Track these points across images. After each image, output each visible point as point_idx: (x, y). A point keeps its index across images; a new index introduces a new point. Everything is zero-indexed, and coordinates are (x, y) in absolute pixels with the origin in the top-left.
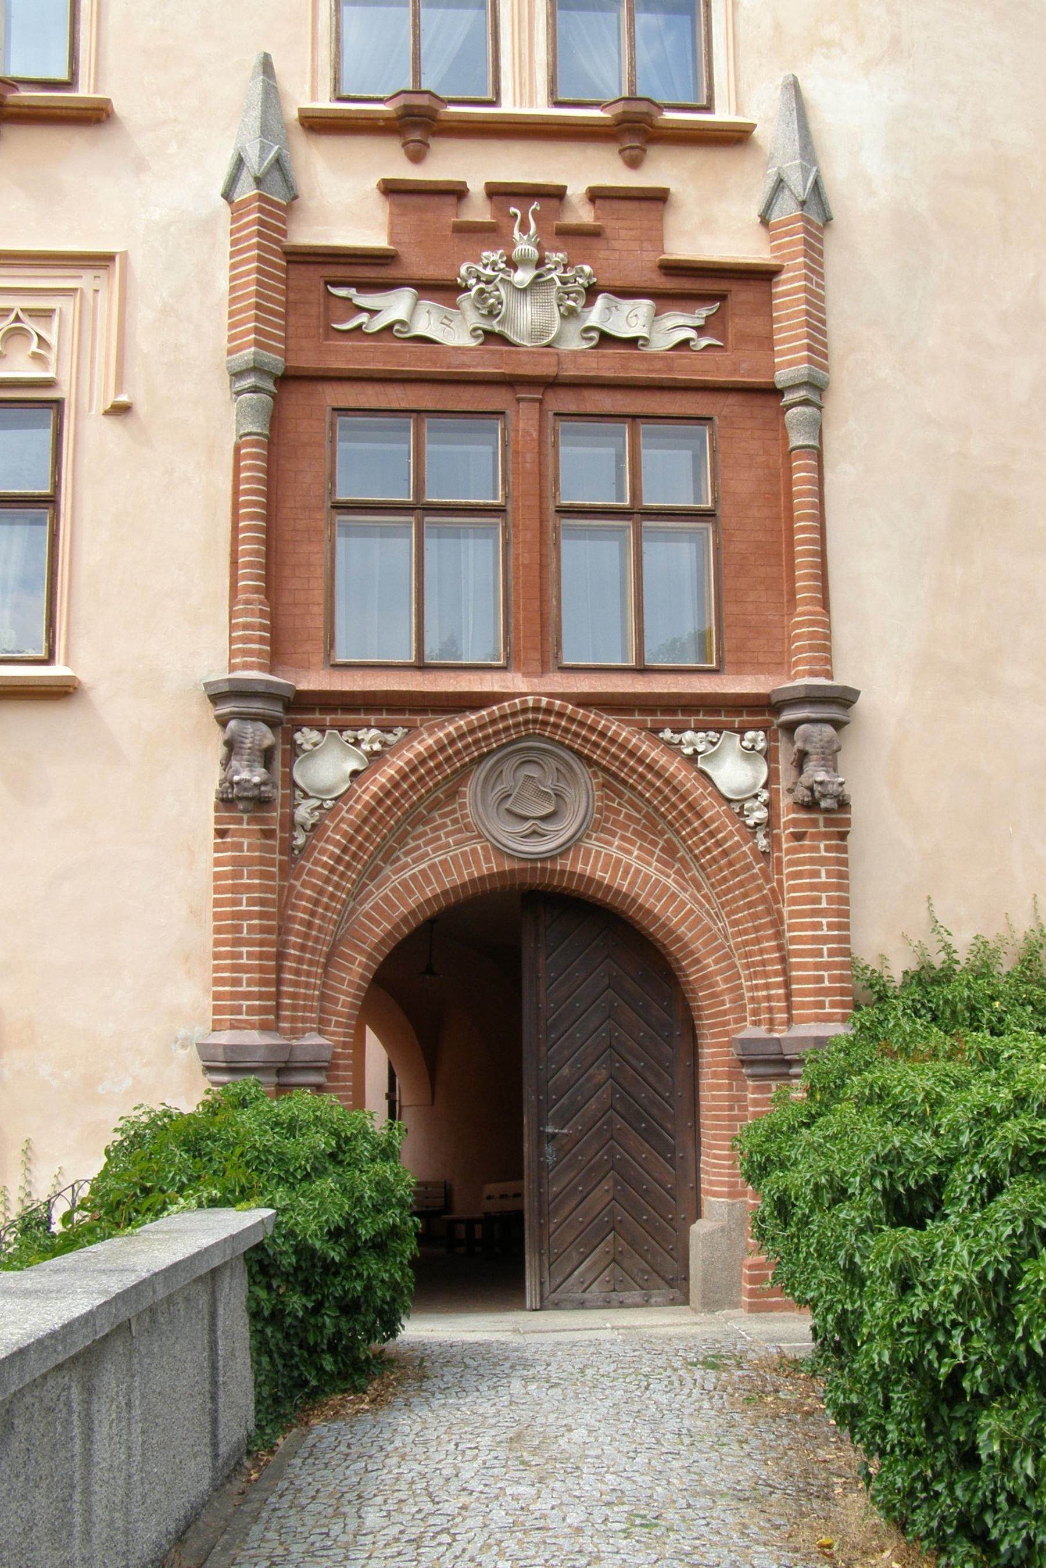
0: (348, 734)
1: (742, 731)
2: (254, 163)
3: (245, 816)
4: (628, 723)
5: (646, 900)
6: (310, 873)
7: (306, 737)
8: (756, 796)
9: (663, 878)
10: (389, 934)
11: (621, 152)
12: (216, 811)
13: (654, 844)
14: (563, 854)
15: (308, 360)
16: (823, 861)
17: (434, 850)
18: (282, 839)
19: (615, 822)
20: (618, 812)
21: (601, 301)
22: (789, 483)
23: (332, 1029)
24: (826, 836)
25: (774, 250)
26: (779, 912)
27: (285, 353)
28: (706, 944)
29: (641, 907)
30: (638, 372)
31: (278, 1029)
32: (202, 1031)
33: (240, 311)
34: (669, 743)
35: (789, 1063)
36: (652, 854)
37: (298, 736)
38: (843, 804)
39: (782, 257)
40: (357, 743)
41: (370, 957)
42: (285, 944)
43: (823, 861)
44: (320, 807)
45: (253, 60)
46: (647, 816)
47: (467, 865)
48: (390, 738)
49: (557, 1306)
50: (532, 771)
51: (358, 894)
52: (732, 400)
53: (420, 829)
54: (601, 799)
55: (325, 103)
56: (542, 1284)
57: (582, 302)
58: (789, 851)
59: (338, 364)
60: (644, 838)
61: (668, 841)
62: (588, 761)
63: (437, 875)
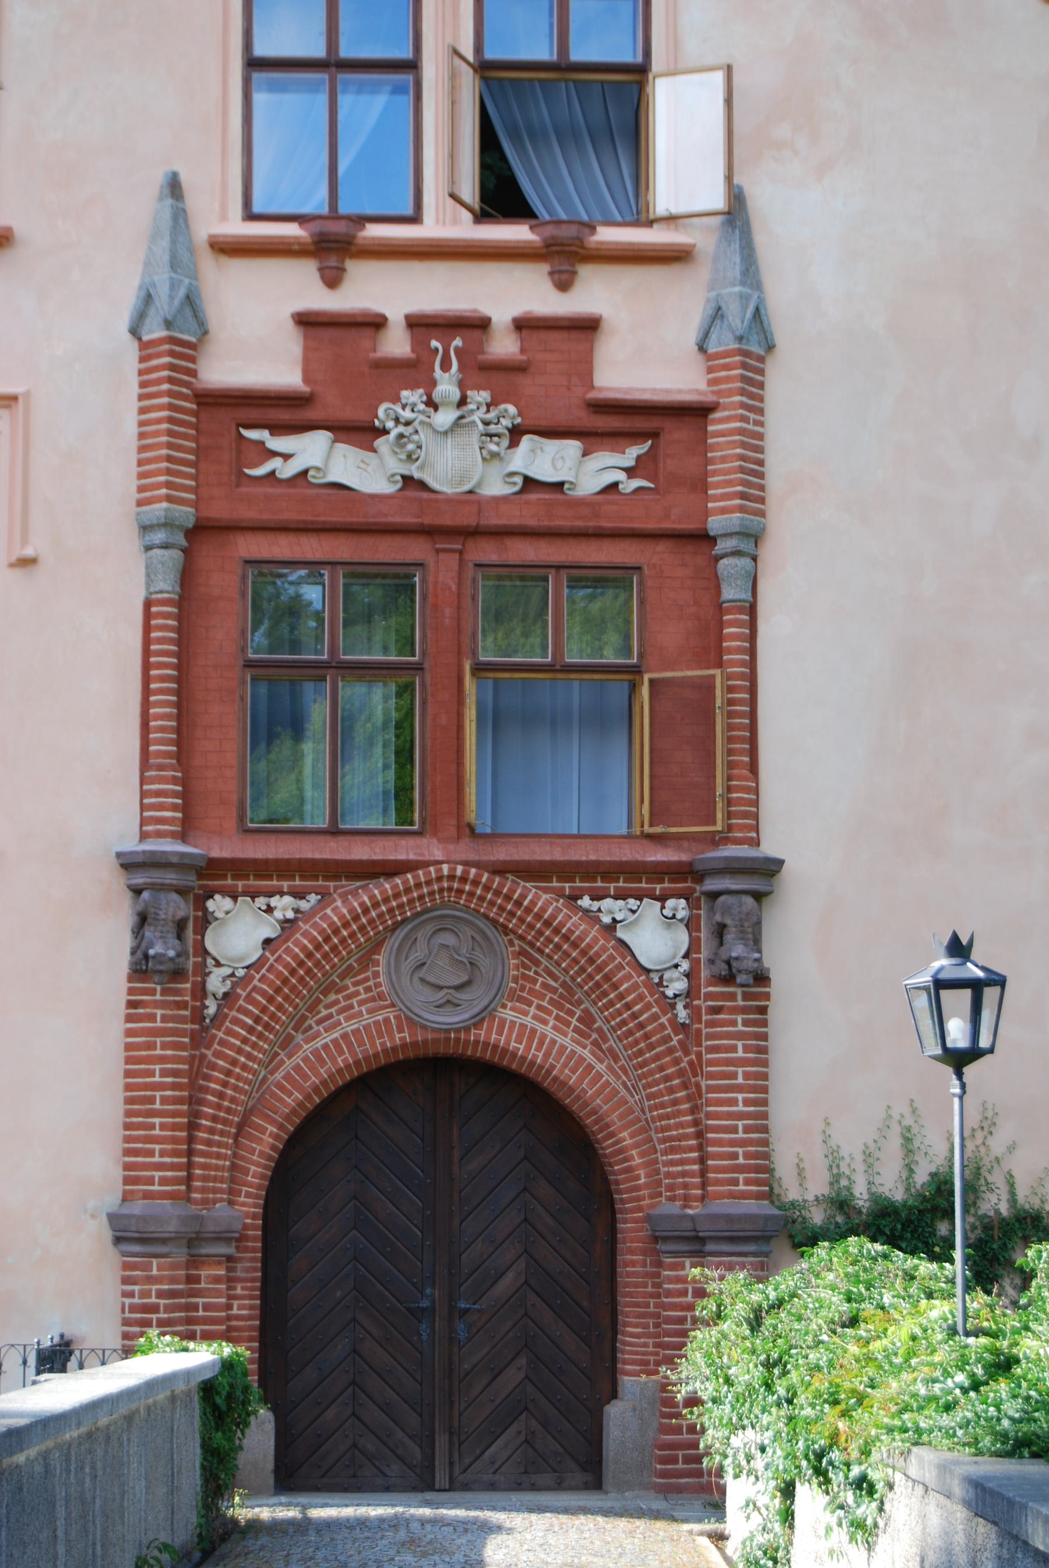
0: (261, 901)
1: (662, 899)
2: (164, 305)
3: (159, 988)
4: (546, 890)
5: (561, 1071)
6: (223, 1043)
7: (219, 904)
8: (676, 966)
9: (579, 1049)
10: (300, 1104)
11: (551, 274)
12: (130, 979)
13: (571, 1013)
14: (477, 1025)
15: (220, 510)
16: (740, 1036)
17: (347, 1019)
18: (194, 1008)
19: (531, 991)
20: (535, 981)
21: (526, 441)
22: (721, 638)
23: (242, 1199)
24: (744, 1010)
25: (711, 382)
26: (698, 1085)
27: (196, 505)
28: (621, 1117)
29: (555, 1079)
30: (563, 521)
31: (189, 1200)
32: (112, 1200)
33: (149, 461)
34: (586, 911)
35: (703, 1241)
36: (568, 1024)
37: (210, 905)
38: (761, 978)
39: (719, 393)
40: (269, 910)
41: (281, 1127)
42: (197, 1115)
43: (740, 1036)
44: (233, 975)
45: (158, 178)
46: (564, 985)
47: (380, 1035)
48: (304, 905)
49: (466, 1487)
50: (448, 939)
51: (272, 1063)
52: (662, 546)
53: (332, 997)
54: (517, 967)
56: (451, 1464)
57: (505, 442)
58: (711, 1024)
60: (560, 1007)
61: (586, 1011)
62: (505, 930)
63: (350, 1045)
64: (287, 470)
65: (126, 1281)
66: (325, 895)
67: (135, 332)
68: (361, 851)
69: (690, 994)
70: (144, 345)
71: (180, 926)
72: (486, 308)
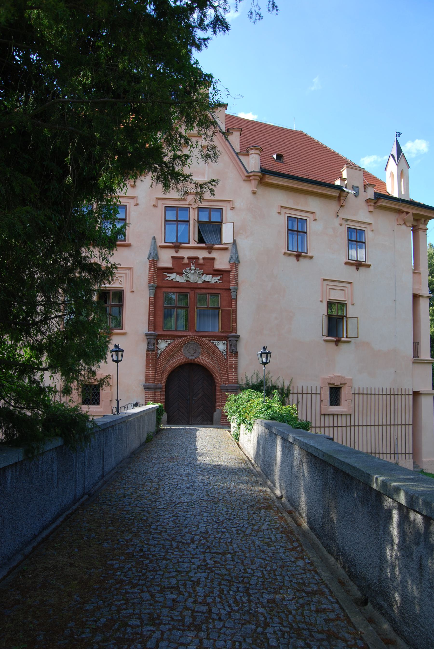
0: (165, 341)
1: (223, 341)
2: (153, 255)
7: (159, 341)
15: (160, 285)
16: (234, 360)
22: (232, 304)
24: (234, 357)
27: (157, 284)
30: (209, 287)
32: (144, 383)
38: (237, 352)
40: (167, 342)
42: (156, 371)
43: (234, 360)
48: (172, 341)
49: (194, 424)
50: (192, 346)
51: (167, 364)
52: (223, 291)
55: (163, 244)
59: (164, 285)
62: (200, 345)
64: (170, 279)
65: (146, 394)
66: (175, 340)
67: (148, 259)
68: (180, 334)
69: (227, 354)
70: (150, 261)
71: (154, 344)
72: (199, 256)
